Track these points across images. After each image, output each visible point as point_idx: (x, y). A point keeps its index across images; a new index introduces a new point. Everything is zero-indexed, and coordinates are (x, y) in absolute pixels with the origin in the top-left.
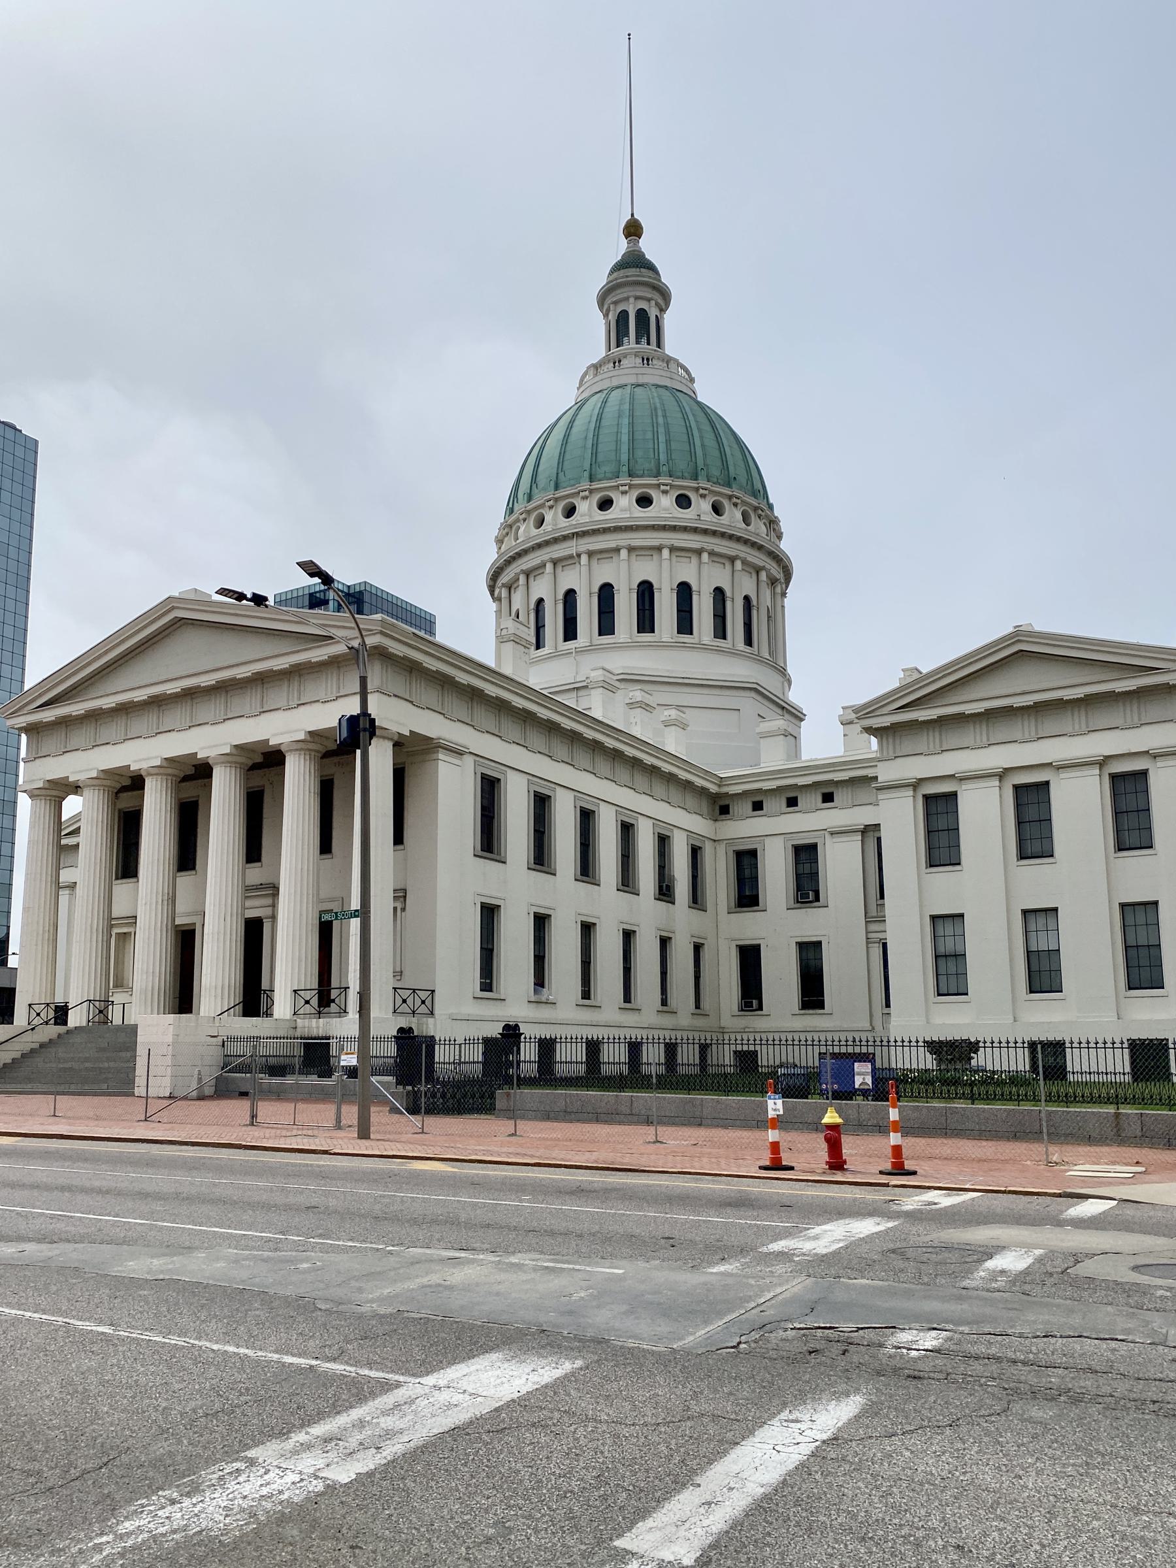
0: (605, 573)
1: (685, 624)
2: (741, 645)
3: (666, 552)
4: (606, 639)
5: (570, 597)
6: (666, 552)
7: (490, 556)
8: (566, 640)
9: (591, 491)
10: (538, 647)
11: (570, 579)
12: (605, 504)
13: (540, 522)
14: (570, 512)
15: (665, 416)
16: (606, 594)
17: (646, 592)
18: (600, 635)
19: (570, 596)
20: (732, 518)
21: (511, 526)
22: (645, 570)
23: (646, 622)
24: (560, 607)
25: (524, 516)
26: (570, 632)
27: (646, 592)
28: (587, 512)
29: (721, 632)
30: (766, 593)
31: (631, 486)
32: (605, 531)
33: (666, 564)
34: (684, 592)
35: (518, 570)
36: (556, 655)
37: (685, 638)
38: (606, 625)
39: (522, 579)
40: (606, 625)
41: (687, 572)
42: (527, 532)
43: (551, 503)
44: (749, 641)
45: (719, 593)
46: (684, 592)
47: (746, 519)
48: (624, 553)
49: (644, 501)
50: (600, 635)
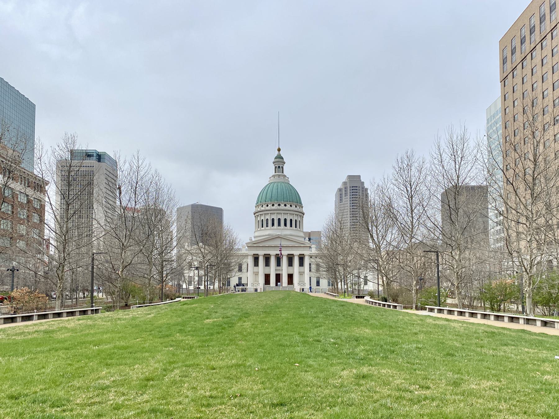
1: (285, 225)
2: (294, 228)
7: (254, 210)
11: (268, 217)
12: (273, 205)
14: (267, 206)
17: (279, 220)
19: (267, 219)
20: (293, 208)
22: (279, 217)
23: (279, 224)
26: (267, 226)
29: (291, 226)
30: (299, 219)
34: (285, 220)
36: (265, 230)
38: (273, 225)
40: (273, 225)
41: (286, 217)
42: (261, 208)
44: (296, 227)
45: (291, 220)
46: (285, 220)
47: (296, 206)
49: (279, 205)
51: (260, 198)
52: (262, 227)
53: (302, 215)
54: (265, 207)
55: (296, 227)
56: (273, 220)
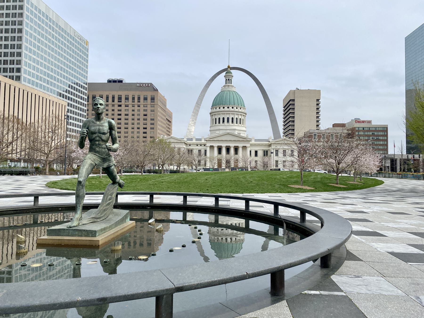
0: (223, 116)
1: (232, 122)
5: (219, 118)
7: (210, 111)
12: (224, 108)
14: (220, 108)
16: (224, 118)
17: (228, 119)
23: (228, 121)
26: (219, 123)
27: (228, 119)
28: (222, 108)
29: (237, 123)
34: (233, 118)
37: (232, 124)
38: (223, 121)
40: (223, 121)
42: (215, 110)
44: (240, 124)
46: (233, 118)
49: (228, 108)
52: (216, 123)
53: (244, 115)
55: (240, 124)
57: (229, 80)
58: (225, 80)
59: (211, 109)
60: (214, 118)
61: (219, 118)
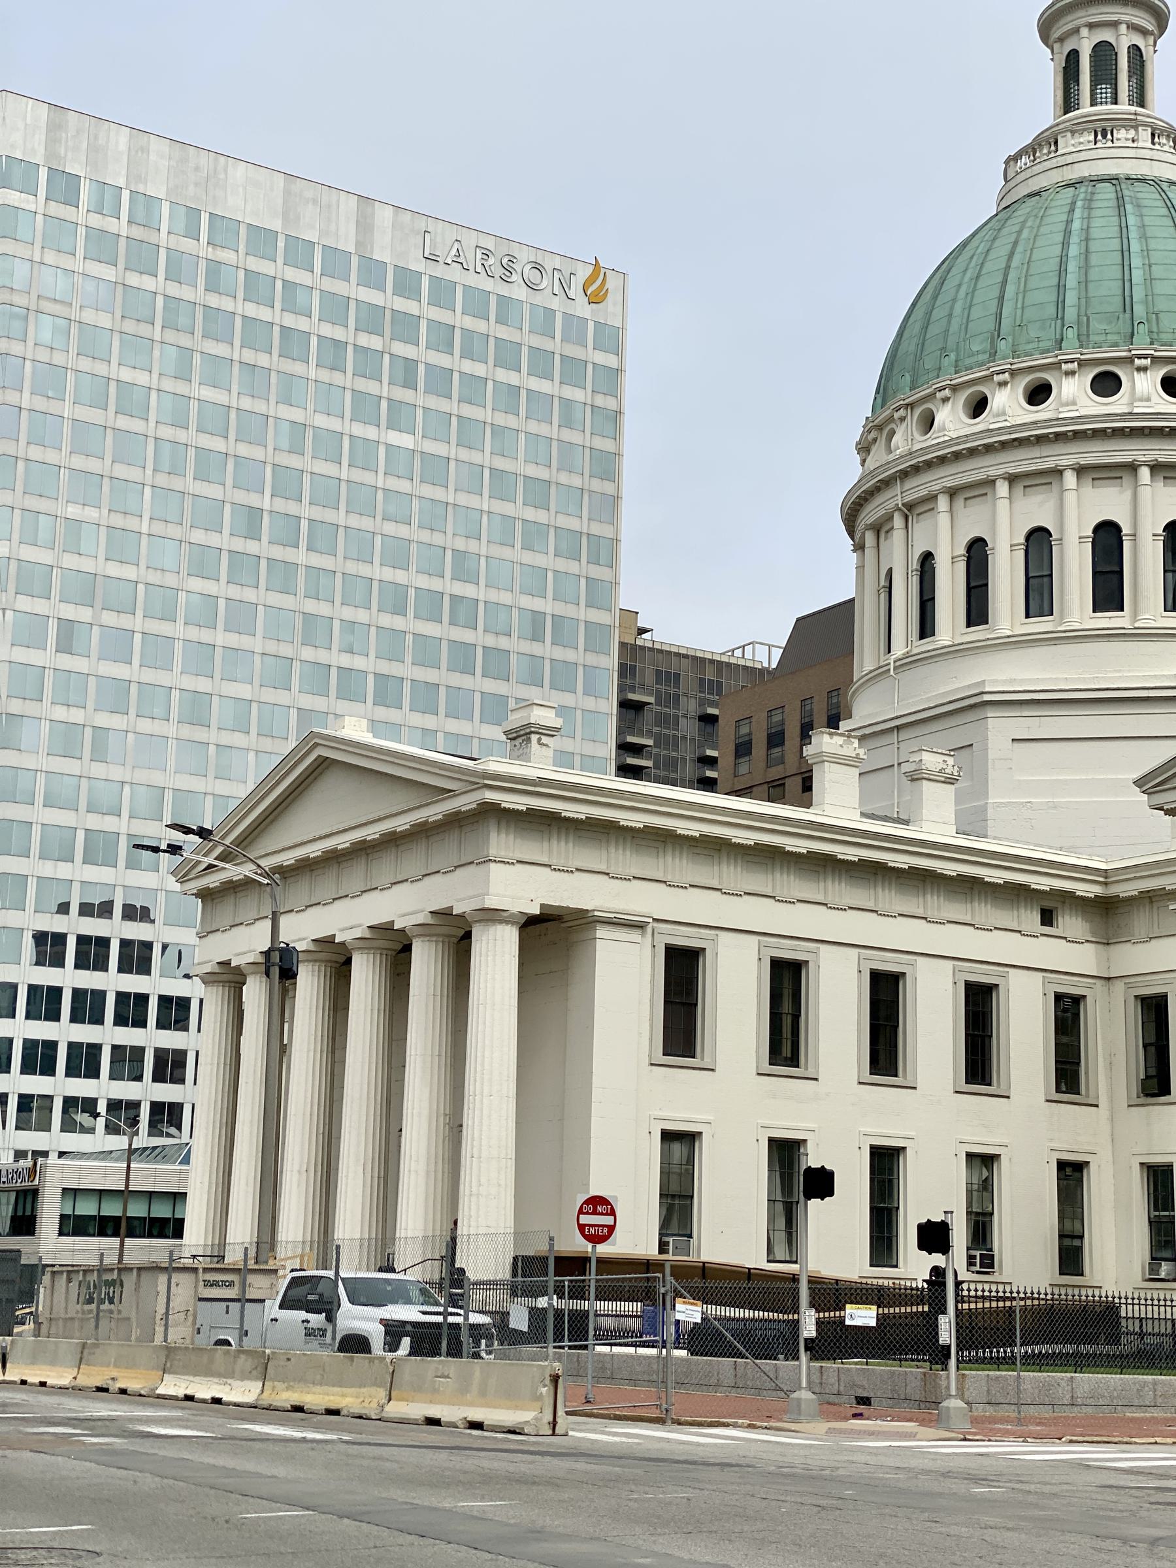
0: (1037, 510)
3: (1145, 472)
4: (1041, 625)
5: (977, 554)
6: (1145, 472)
8: (969, 625)
9: (1013, 373)
10: (922, 637)
12: (1038, 394)
13: (928, 422)
14: (979, 407)
15: (1144, 237)
17: (1108, 540)
18: (1027, 616)
21: (880, 428)
24: (962, 566)
25: (902, 412)
26: (977, 610)
27: (1108, 540)
28: (1009, 406)
31: (1082, 363)
32: (1040, 440)
33: (1145, 493)
35: (891, 505)
38: (1039, 595)
39: (898, 521)
40: (1039, 595)
42: (906, 441)
43: (947, 392)
48: (1070, 478)
49: (1106, 384)
50: (1027, 616)
51: (915, 328)
52: (926, 628)
54: (952, 421)
56: (1038, 541)
57: (1104, 54)
58: (1044, 69)
59: (864, 449)
60: (899, 556)
61: (977, 554)
